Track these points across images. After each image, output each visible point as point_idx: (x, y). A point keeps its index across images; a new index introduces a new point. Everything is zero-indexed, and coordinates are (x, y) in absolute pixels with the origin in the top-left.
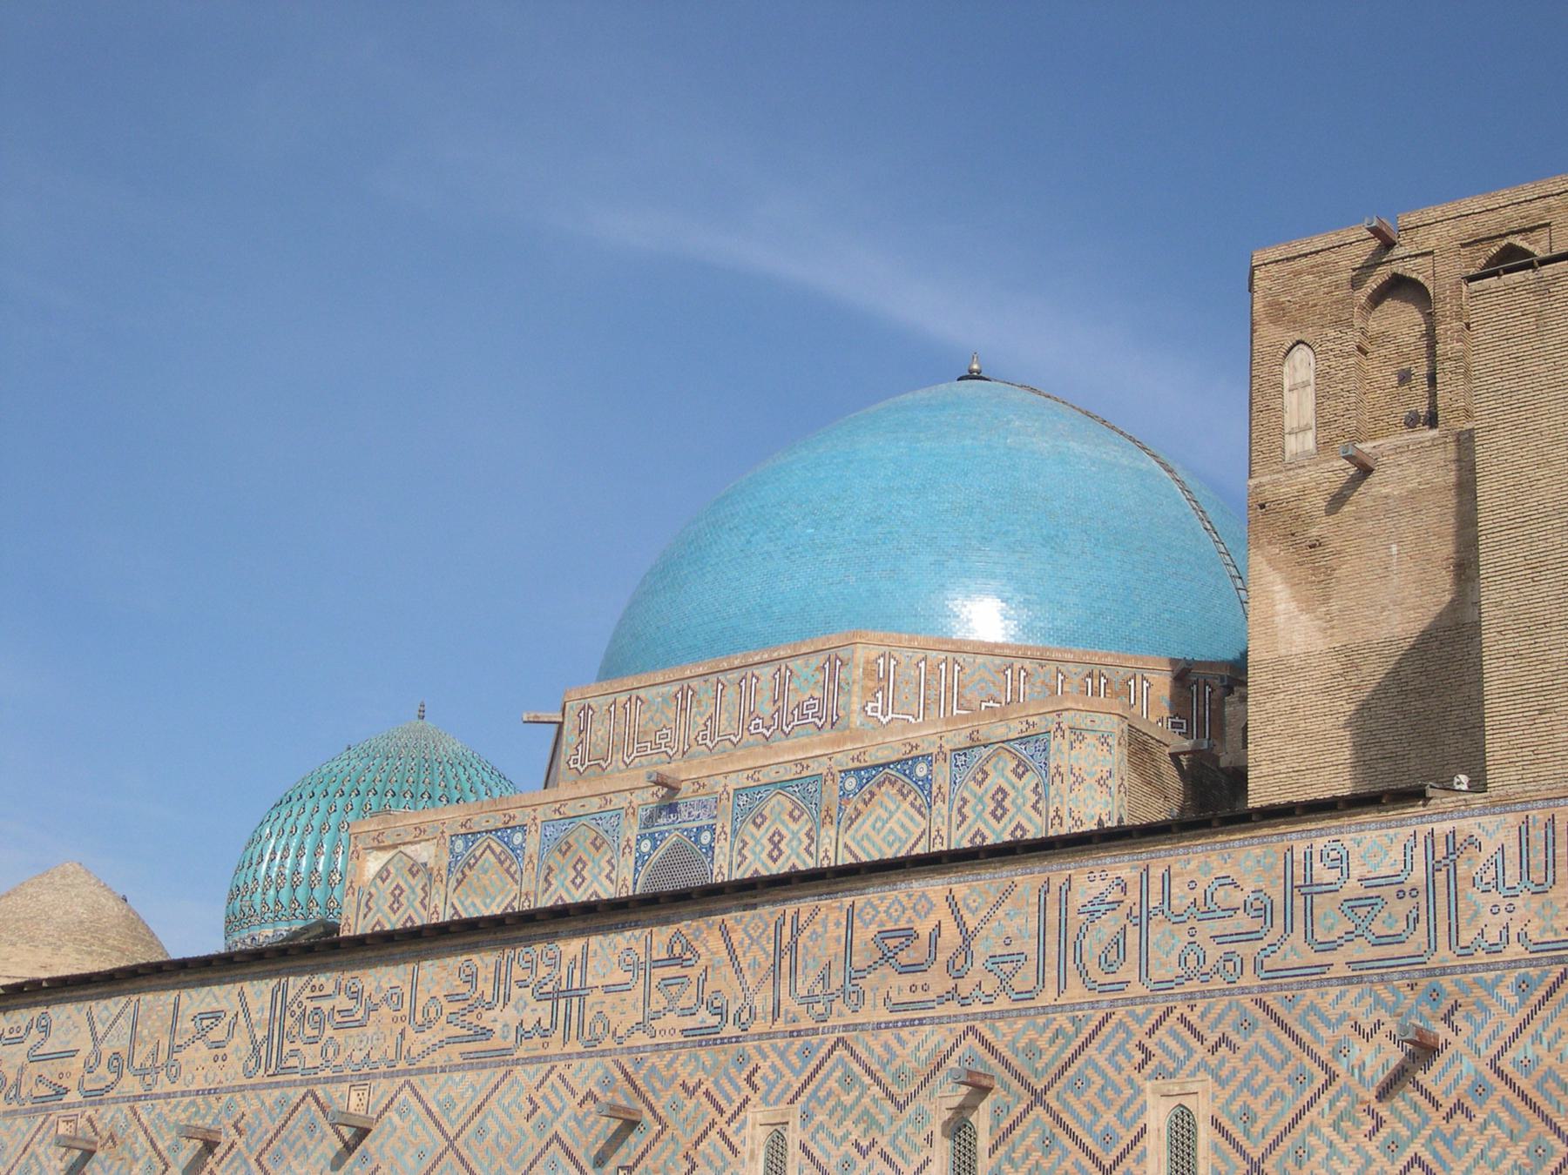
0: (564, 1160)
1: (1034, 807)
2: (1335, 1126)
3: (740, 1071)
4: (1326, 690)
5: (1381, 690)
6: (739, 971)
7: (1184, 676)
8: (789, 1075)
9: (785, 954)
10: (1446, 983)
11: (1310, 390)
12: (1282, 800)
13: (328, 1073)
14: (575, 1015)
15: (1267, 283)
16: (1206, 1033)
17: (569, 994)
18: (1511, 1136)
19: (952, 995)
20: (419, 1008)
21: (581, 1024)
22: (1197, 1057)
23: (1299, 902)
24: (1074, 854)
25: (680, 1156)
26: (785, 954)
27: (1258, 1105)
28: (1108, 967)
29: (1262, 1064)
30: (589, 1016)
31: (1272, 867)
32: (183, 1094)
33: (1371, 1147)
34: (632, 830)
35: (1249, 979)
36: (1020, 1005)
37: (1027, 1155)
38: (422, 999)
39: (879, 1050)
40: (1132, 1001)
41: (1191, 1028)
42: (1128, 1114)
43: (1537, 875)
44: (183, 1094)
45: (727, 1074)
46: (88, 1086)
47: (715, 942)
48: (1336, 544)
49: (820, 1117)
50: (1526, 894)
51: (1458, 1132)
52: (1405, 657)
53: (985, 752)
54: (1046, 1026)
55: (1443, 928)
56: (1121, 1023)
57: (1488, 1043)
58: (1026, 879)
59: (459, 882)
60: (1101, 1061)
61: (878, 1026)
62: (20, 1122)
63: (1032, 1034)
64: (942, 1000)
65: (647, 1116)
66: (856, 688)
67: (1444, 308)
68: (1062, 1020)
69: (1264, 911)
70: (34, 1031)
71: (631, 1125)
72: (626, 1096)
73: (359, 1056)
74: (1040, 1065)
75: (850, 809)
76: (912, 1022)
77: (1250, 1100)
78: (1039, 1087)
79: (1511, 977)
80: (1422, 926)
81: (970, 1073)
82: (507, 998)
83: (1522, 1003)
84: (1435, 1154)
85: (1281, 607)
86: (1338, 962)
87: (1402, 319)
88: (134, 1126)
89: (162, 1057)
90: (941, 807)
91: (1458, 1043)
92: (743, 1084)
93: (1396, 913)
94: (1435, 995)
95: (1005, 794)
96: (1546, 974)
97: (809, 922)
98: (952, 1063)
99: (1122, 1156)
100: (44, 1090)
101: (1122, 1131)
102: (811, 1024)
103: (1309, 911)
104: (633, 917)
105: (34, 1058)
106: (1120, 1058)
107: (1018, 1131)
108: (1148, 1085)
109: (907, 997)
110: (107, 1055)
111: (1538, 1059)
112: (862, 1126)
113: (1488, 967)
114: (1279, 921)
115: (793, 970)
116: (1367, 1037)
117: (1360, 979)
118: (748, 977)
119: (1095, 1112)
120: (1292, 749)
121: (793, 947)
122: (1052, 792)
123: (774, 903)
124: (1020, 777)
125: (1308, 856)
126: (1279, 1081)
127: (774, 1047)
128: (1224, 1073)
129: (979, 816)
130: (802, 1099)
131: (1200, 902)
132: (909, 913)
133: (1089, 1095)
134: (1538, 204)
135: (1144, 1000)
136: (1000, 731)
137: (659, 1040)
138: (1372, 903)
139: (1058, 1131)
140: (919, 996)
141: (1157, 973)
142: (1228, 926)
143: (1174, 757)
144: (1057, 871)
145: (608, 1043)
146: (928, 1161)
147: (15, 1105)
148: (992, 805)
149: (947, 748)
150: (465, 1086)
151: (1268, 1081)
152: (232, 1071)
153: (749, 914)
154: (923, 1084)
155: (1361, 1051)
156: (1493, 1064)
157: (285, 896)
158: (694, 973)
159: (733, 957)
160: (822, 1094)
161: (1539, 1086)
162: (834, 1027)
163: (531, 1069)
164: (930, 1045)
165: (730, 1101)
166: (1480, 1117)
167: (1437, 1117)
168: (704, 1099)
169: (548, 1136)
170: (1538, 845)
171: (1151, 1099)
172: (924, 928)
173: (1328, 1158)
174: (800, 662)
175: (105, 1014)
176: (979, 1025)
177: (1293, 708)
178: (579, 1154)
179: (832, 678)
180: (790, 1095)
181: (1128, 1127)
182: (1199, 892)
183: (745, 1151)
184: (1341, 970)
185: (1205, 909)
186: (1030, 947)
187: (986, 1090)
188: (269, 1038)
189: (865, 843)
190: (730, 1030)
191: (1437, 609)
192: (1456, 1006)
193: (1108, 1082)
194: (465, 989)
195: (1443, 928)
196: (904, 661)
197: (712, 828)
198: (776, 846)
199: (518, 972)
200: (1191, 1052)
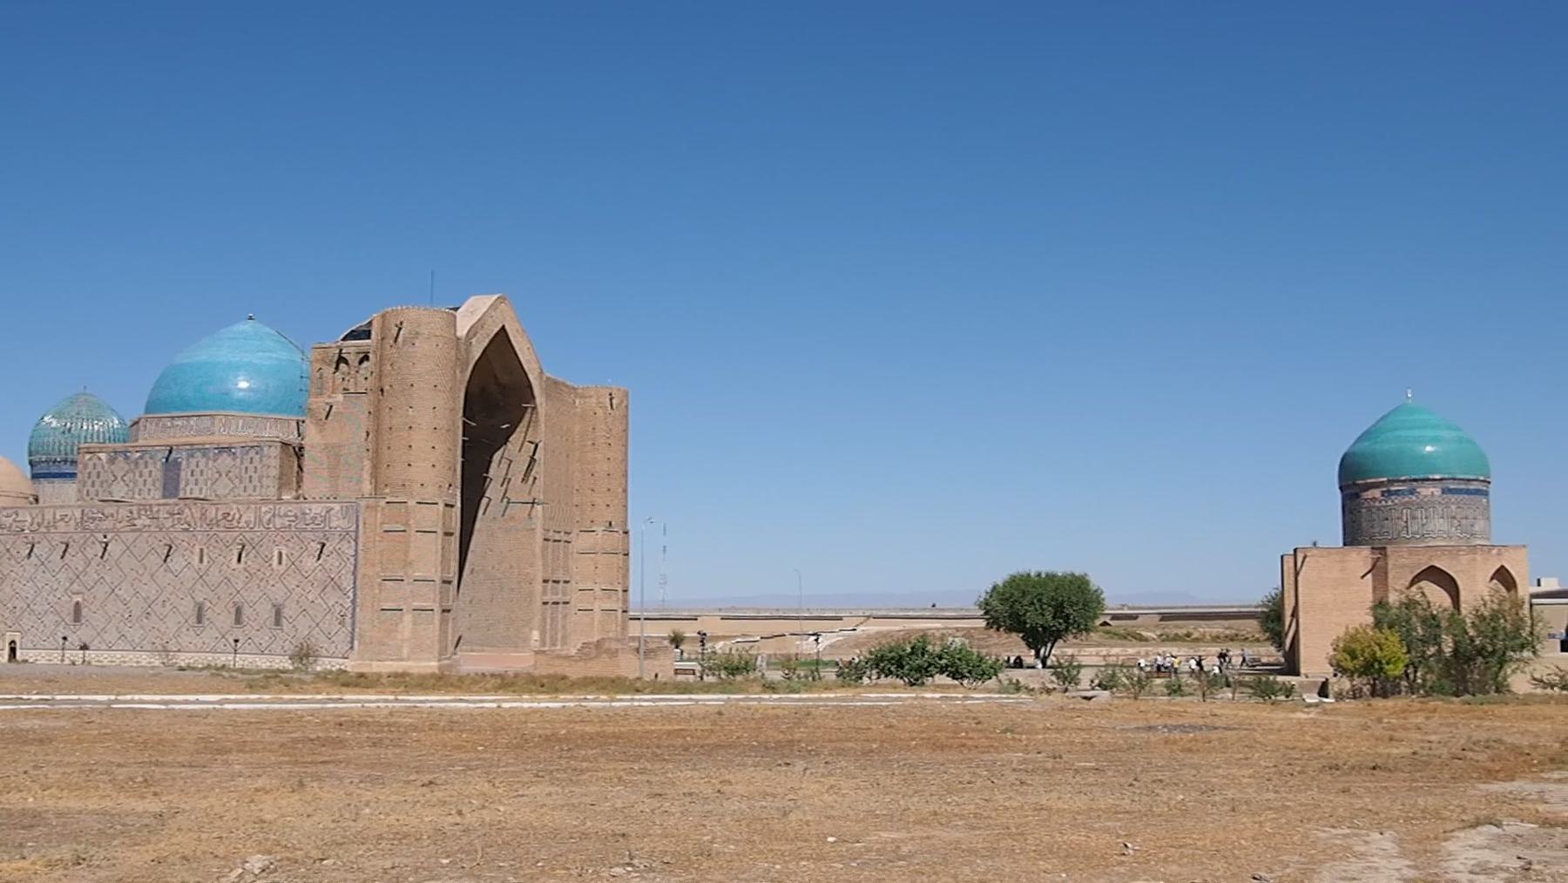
69: (296, 516)
71: (171, 547)
86: (309, 528)
90: (238, 460)
105: (15, 521)
126: (298, 548)
155: (312, 544)
158: (183, 517)
172: (232, 513)
186: (253, 519)
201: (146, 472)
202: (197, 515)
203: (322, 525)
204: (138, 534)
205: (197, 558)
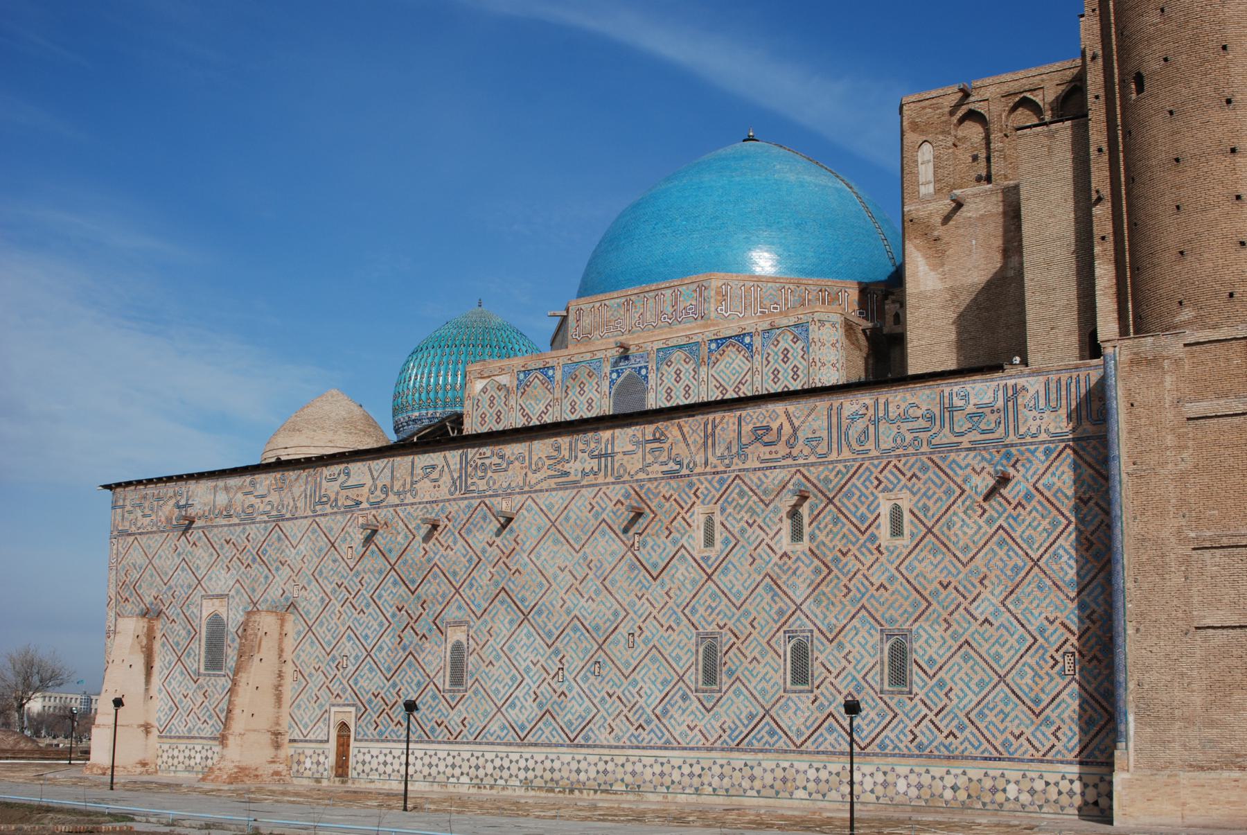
0: (609, 531)
1: (802, 357)
2: (965, 512)
3: (691, 490)
4: (943, 307)
5: (969, 307)
6: (688, 445)
7: (865, 290)
8: (714, 492)
9: (709, 438)
10: (1013, 450)
11: (931, 164)
12: (939, 370)
13: (491, 493)
14: (609, 465)
15: (909, 112)
16: (906, 472)
17: (606, 455)
18: (1042, 516)
19: (789, 455)
20: (533, 462)
21: (613, 469)
22: (902, 483)
23: (947, 414)
24: (843, 392)
25: (664, 528)
26: (709, 438)
27: (930, 503)
28: (861, 443)
29: (932, 486)
30: (616, 466)
31: (934, 399)
32: (420, 503)
33: (981, 522)
34: (607, 368)
35: (925, 449)
36: (820, 460)
37: (826, 526)
38: (535, 458)
39: (755, 480)
40: (872, 458)
41: (899, 470)
42: (872, 508)
43: (1053, 404)
44: (420, 503)
45: (684, 490)
46: (372, 501)
47: (676, 432)
48: (947, 239)
49: (730, 510)
50: (1048, 412)
51: (1019, 515)
52: (980, 292)
53: (778, 332)
54: (833, 469)
55: (1011, 427)
57: (1032, 476)
58: (822, 404)
59: (523, 393)
60: (859, 484)
61: (755, 469)
62: (339, 517)
63: (826, 473)
64: (784, 458)
65: (647, 510)
66: (712, 300)
67: (994, 127)
68: (840, 467)
69: (931, 419)
70: (342, 475)
71: (639, 515)
72: (636, 501)
73: (505, 485)
74: (831, 486)
75: (713, 358)
76: (771, 468)
77: (927, 502)
78: (831, 496)
79: (1042, 448)
80: (1002, 425)
81: (801, 491)
82: (576, 457)
83: (1047, 459)
84: (1009, 524)
85: (921, 268)
86: (965, 441)
87: (973, 131)
88: (397, 519)
89: (408, 486)
91: (1019, 476)
92: (692, 496)
94: (1008, 456)
95: (788, 352)
96: (1057, 446)
97: (720, 423)
98: (790, 486)
99: (870, 526)
100: (350, 503)
101: (869, 515)
102: (723, 469)
103: (952, 419)
104: (636, 421)
106: (867, 483)
107: (822, 516)
108: (880, 495)
109: (768, 456)
110: (380, 485)
111: (1054, 484)
112: (749, 514)
113: (1031, 444)
114: (938, 423)
115: (714, 445)
116: (979, 474)
117: (975, 449)
118: (692, 448)
119: (856, 507)
120: (928, 334)
121: (713, 434)
122: (811, 350)
123: (703, 414)
124: (795, 343)
125: (951, 394)
126: (939, 493)
127: (706, 479)
128: (915, 490)
129: (776, 361)
130: (721, 502)
131: (902, 414)
132: (767, 419)
133: (854, 499)
134: (1038, 78)
135: (877, 458)
136: (785, 322)
137: (651, 476)
138: (980, 415)
139: (840, 515)
140: (774, 456)
141: (883, 446)
142: (915, 425)
143: (864, 331)
144: (836, 401)
145: (626, 477)
146: (780, 529)
147: (335, 510)
148: (782, 356)
149: (759, 329)
150: (559, 498)
151: (934, 493)
152: (443, 492)
153: (691, 419)
154: (777, 495)
155: (976, 480)
156: (1034, 485)
157: (424, 397)
158: (666, 446)
159: (685, 439)
160: (730, 500)
161: (1055, 495)
162: (734, 471)
163: (590, 489)
164: (780, 477)
165: (686, 503)
166: (1029, 509)
167: (1010, 509)
168: (674, 503)
169: (600, 520)
170: (1053, 389)
171: (881, 501)
172: (775, 426)
173: (962, 526)
174: (684, 287)
175: (377, 467)
176: (801, 469)
177: (928, 315)
178: (615, 527)
179: (700, 295)
180: (714, 501)
181: (872, 513)
182: (901, 410)
183: (694, 525)
185: (905, 418)
186: (825, 434)
187: (806, 498)
188: (460, 477)
189: (721, 374)
190: (685, 471)
191: (994, 270)
192: (1017, 461)
193: (862, 494)
194: (555, 453)
195: (1011, 427)
196: (734, 287)
197: (646, 368)
198: (678, 375)
199: (581, 446)
200: (899, 481)
202: (698, 438)
204: (569, 493)
205: (700, 535)
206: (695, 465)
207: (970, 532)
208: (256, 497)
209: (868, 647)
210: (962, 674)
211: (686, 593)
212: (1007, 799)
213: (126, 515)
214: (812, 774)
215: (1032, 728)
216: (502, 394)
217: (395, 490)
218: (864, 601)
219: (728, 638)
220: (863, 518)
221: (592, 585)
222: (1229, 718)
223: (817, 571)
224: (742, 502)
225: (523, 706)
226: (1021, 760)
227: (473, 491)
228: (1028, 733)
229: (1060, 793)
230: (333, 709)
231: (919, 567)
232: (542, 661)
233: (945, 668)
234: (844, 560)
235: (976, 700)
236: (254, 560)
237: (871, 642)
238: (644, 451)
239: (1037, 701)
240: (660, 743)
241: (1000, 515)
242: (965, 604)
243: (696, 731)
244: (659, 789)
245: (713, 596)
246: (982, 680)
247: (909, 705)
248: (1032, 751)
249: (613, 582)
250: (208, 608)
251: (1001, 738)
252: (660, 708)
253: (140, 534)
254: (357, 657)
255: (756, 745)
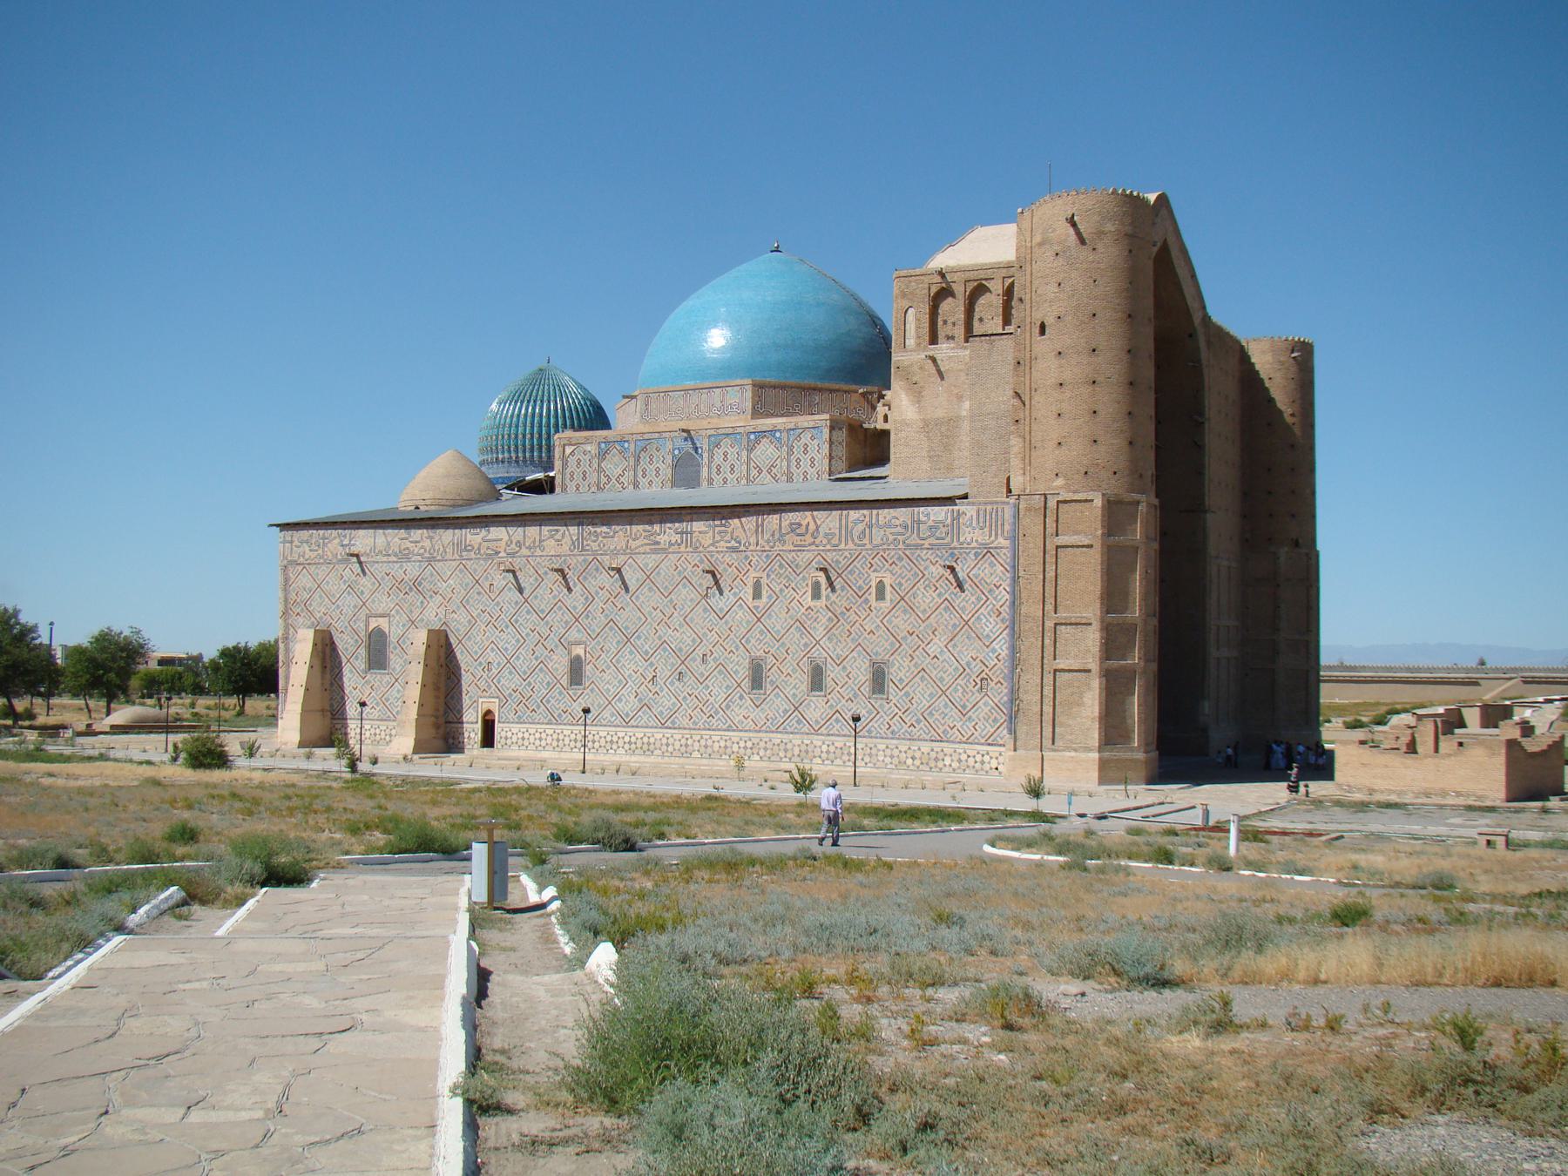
10: (956, 551)
17: (687, 533)
19: (813, 543)
27: (903, 581)
28: (859, 538)
35: (901, 546)
49: (773, 576)
56: (864, 556)
60: (858, 566)
64: (810, 545)
68: (847, 553)
73: (612, 547)
86: (926, 544)
89: (537, 543)
93: (941, 532)
94: (952, 555)
100: (490, 552)
103: (919, 528)
109: (799, 543)
115: (762, 531)
129: (799, 452)
141: (874, 543)
142: (893, 530)
150: (651, 560)
155: (932, 568)
158: (730, 530)
159: (743, 527)
161: (980, 582)
170: (981, 516)
172: (804, 523)
184: (927, 546)
186: (837, 532)
190: (742, 548)
201: (651, 469)
203: (948, 539)
205: (750, 591)
206: (750, 544)
207: (927, 601)
208: (412, 542)
209: (862, 670)
210: (919, 689)
211: (742, 629)
212: (945, 765)
213: (295, 549)
214: (825, 748)
215: (961, 723)
216: (587, 457)
217: (527, 544)
218: (860, 641)
219: (771, 660)
220: (860, 588)
221: (676, 620)
222: (1071, 722)
223: (830, 619)
224: (781, 572)
225: (627, 701)
226: (953, 742)
227: (588, 550)
228: (958, 725)
229: (976, 762)
230: (481, 700)
231: (896, 621)
232: (641, 670)
233: (911, 684)
234: (848, 614)
235: (928, 705)
236: (411, 589)
237: (864, 667)
238: (714, 532)
239: (964, 706)
240: (724, 727)
241: (946, 592)
242: (923, 645)
243: (749, 720)
244: (724, 757)
245: (761, 632)
246: (932, 693)
247: (888, 706)
248: (960, 736)
249: (691, 619)
250: (373, 624)
251: (942, 729)
252: (724, 704)
253: (309, 564)
254: (499, 664)
255: (789, 730)
